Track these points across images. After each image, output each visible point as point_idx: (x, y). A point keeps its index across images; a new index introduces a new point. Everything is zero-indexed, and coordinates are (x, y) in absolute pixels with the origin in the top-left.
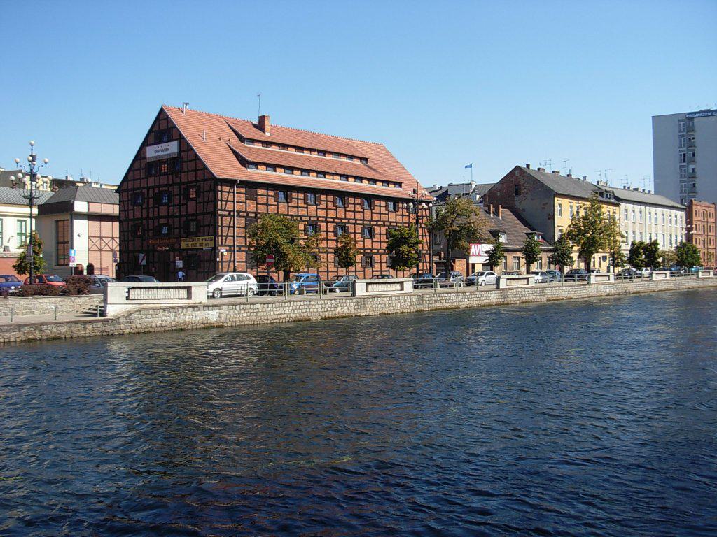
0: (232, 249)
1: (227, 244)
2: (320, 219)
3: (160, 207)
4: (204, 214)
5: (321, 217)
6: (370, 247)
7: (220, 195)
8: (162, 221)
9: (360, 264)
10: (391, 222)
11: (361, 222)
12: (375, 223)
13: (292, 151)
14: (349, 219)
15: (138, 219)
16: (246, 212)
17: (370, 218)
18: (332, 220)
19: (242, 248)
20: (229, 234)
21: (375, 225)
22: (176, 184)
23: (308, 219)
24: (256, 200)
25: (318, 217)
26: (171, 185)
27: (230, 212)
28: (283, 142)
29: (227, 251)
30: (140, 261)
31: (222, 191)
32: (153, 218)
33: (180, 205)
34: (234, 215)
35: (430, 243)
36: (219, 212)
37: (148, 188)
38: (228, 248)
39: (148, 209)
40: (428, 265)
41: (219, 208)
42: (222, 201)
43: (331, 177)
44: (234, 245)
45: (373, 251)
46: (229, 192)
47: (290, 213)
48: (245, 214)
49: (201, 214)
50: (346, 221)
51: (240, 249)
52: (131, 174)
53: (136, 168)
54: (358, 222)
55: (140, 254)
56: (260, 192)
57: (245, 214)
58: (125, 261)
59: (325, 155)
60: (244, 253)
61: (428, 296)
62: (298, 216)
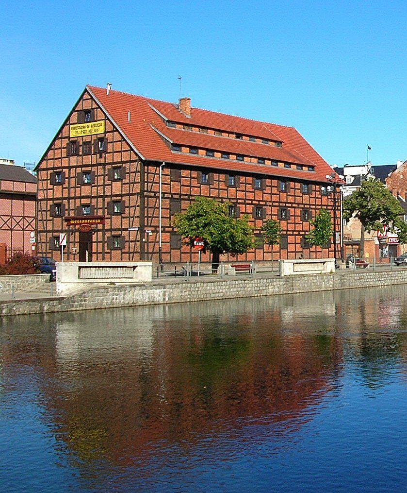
0: (156, 231)
2: (239, 201)
3: (82, 187)
4: (129, 195)
5: (240, 199)
6: (286, 229)
7: (146, 177)
8: (84, 201)
10: (305, 204)
11: (277, 204)
12: (290, 205)
13: (211, 133)
14: (266, 202)
15: (58, 199)
16: (170, 193)
17: (285, 200)
18: (250, 202)
19: (167, 229)
20: (154, 216)
21: (289, 207)
22: (100, 165)
24: (180, 182)
26: (94, 165)
27: (156, 193)
28: (203, 125)
29: (152, 232)
30: (61, 241)
31: (148, 173)
32: (75, 198)
33: (104, 185)
34: (159, 197)
35: (340, 225)
37: (69, 168)
39: (69, 188)
41: (145, 189)
44: (159, 227)
47: (211, 195)
48: (170, 196)
49: (126, 195)
50: (264, 203)
51: (164, 230)
52: (51, 152)
53: (56, 147)
54: (274, 204)
55: (61, 234)
56: (185, 173)
58: (43, 241)
60: (169, 234)
62: (219, 198)
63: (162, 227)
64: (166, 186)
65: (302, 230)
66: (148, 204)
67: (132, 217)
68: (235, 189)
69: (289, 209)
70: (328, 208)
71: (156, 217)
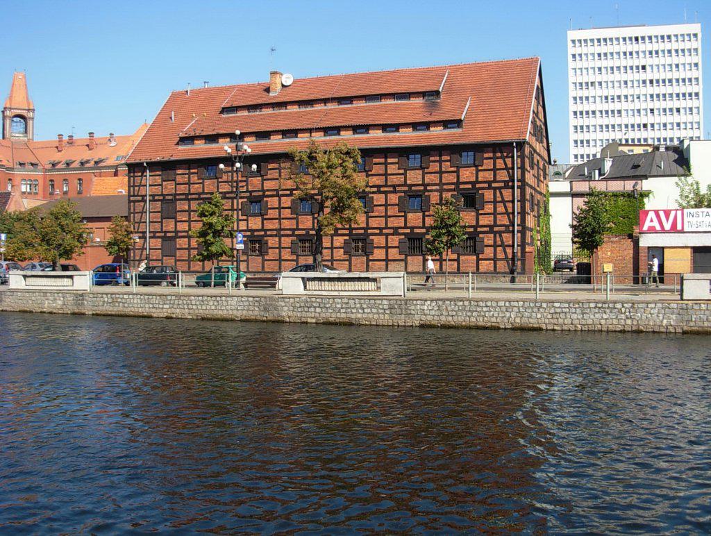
1: (140, 230)
2: (267, 193)
5: (268, 190)
6: (364, 225)
9: (342, 250)
16: (162, 195)
18: (288, 192)
19: (158, 235)
21: (373, 193)
23: (248, 194)
25: (264, 191)
29: (140, 238)
36: (132, 198)
38: (141, 235)
40: (509, 251)
41: (132, 194)
42: (134, 186)
43: (308, 135)
45: (370, 231)
46: (142, 176)
48: (161, 198)
57: (161, 198)
59: (351, 103)
60: (160, 240)
61: (91, 296)
63: (150, 232)
64: (156, 187)
65: (403, 225)
66: (134, 210)
67: (137, 223)
68: (260, 178)
69: (371, 195)
70: (477, 186)
71: (143, 222)
